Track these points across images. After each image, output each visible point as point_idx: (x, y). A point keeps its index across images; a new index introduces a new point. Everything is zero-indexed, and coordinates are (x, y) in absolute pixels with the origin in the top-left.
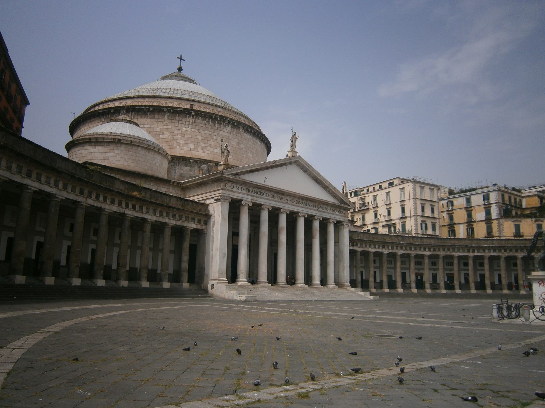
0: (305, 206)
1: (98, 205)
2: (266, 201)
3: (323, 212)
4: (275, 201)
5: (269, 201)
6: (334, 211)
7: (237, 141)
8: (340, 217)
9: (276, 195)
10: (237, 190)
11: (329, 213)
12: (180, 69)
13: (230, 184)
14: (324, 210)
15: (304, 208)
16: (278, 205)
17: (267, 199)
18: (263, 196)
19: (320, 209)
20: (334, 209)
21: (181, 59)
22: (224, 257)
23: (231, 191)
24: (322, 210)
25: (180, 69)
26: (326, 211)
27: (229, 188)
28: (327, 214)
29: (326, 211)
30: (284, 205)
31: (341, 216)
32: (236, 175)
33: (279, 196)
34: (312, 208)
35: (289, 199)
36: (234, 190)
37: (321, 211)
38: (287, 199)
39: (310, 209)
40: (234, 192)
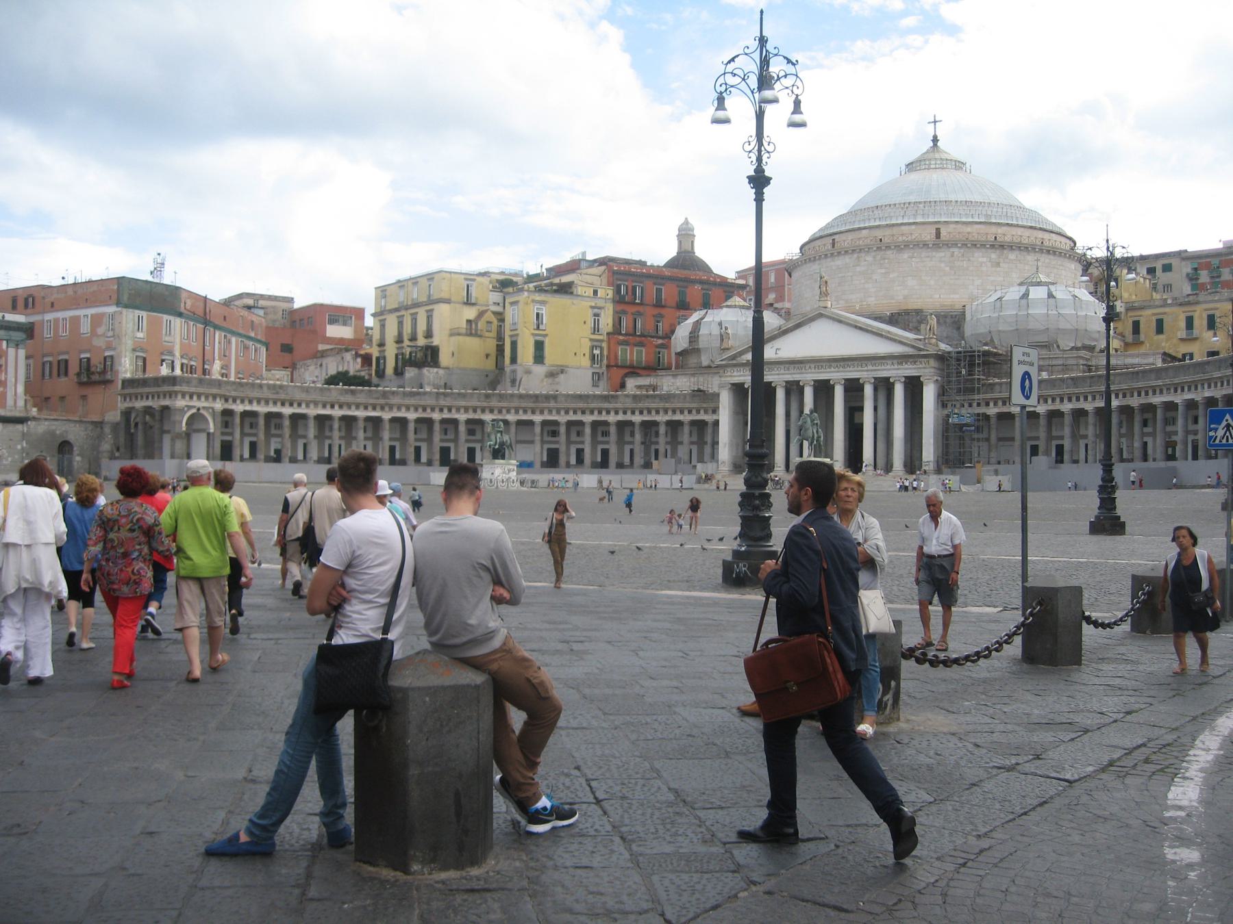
0: (841, 369)
1: (603, 418)
2: (776, 377)
3: (875, 370)
4: (791, 374)
5: (781, 376)
6: (901, 363)
7: (883, 271)
8: (916, 371)
9: (792, 366)
10: (739, 374)
11: (889, 370)
12: (935, 140)
13: (729, 370)
14: (879, 368)
15: (838, 372)
16: (796, 377)
17: (778, 374)
18: (773, 372)
19: (870, 367)
20: (900, 361)
21: (935, 122)
22: (725, 446)
23: (731, 376)
24: (874, 368)
25: (935, 140)
26: (883, 367)
27: (729, 374)
28: (885, 372)
29: (883, 367)
30: (805, 375)
31: (915, 368)
32: (734, 357)
33: (797, 366)
34: (856, 368)
35: (813, 366)
36: (735, 374)
37: (872, 370)
38: (810, 367)
39: (850, 371)
40: (734, 376)
